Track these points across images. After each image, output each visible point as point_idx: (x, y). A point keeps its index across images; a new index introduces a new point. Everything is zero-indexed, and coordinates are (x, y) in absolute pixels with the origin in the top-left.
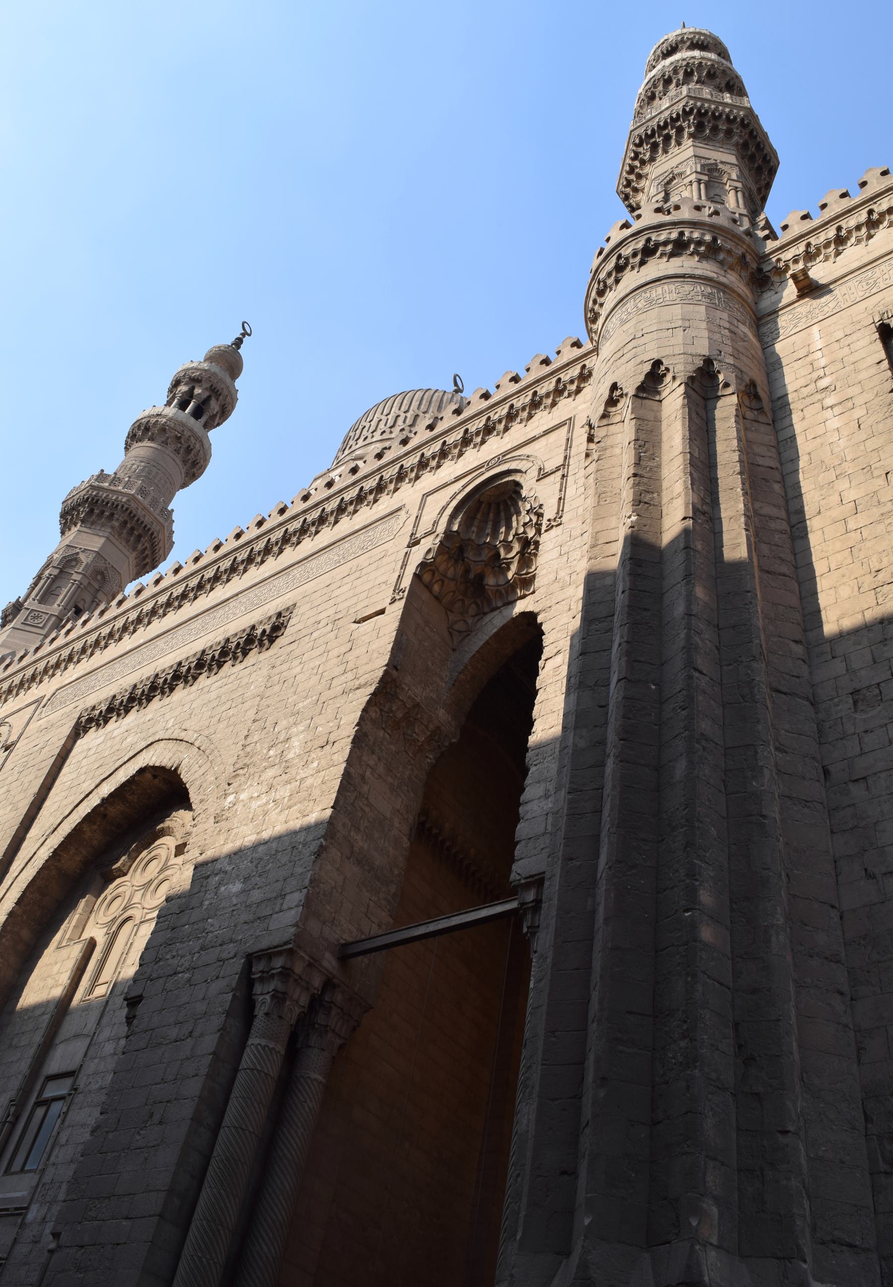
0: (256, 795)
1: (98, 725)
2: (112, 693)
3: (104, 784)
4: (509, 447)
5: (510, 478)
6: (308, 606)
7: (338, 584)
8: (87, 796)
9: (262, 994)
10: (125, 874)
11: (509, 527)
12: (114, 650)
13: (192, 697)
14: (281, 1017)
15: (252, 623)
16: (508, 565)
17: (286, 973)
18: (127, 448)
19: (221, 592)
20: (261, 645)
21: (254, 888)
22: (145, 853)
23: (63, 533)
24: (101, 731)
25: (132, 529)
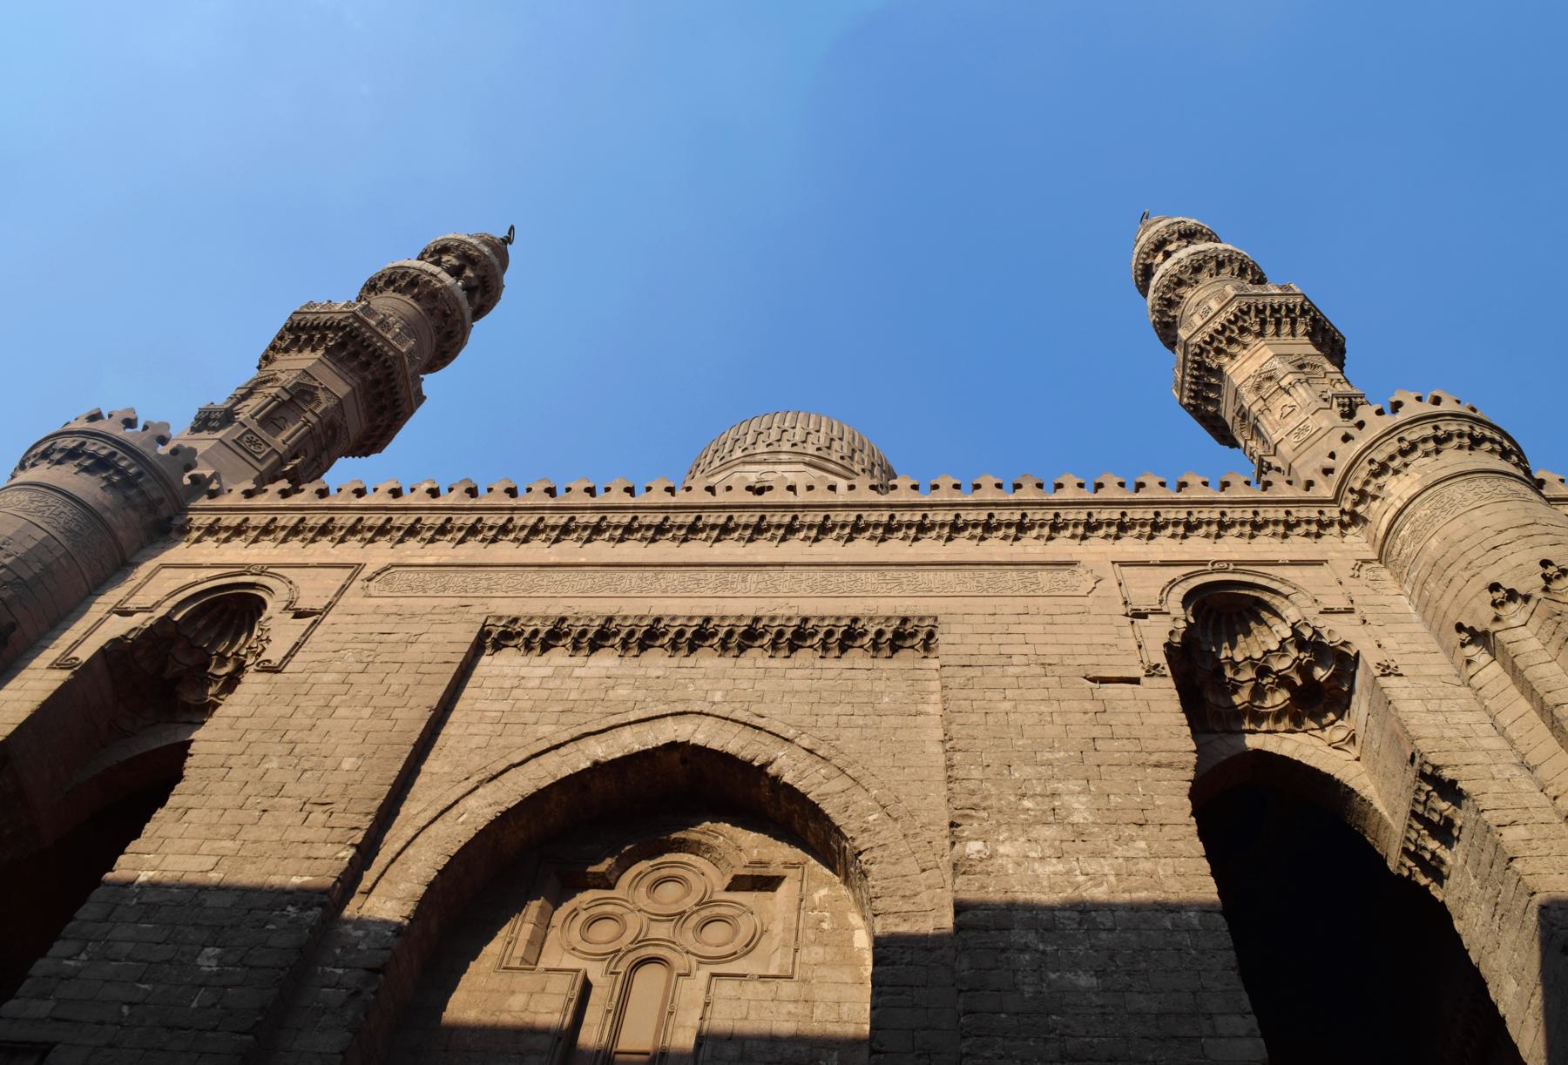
3: (591, 741)
4: (1236, 557)
10: (611, 887)
11: (1232, 647)
16: (1236, 688)
18: (371, 287)
22: (644, 865)
25: (381, 395)
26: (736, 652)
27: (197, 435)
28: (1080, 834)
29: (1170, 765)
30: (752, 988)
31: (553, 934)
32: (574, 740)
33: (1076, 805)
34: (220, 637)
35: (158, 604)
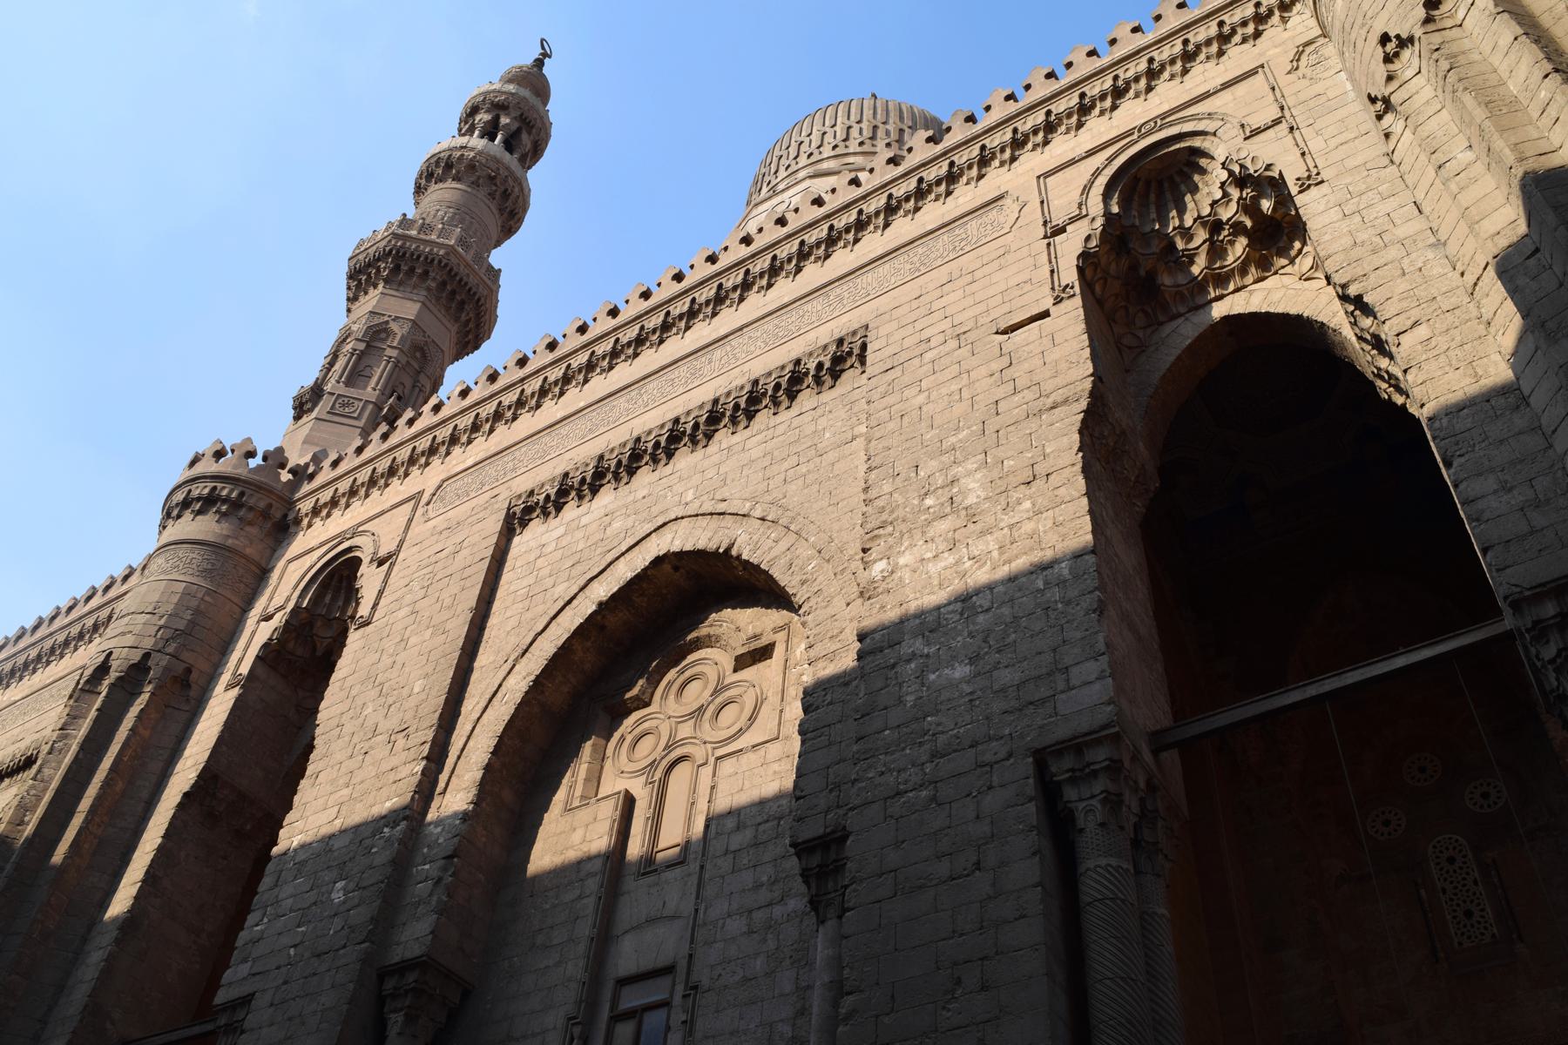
0: (929, 555)
2: (560, 471)
3: (595, 584)
4: (1166, 108)
5: (1182, 145)
6: (894, 325)
7: (938, 293)
8: (569, 602)
9: (1081, 800)
10: (648, 704)
11: (1182, 211)
12: (527, 422)
14: (1122, 828)
15: (794, 355)
17: (1114, 768)
18: (419, 190)
19: (702, 332)
20: (818, 380)
21: (996, 668)
23: (352, 300)
24: (553, 522)
25: (453, 293)
26: (704, 442)
27: (301, 422)
28: (972, 516)
29: (1066, 401)
30: (751, 759)
31: (608, 764)
32: (582, 589)
33: (972, 486)
34: (347, 602)
35: (288, 599)
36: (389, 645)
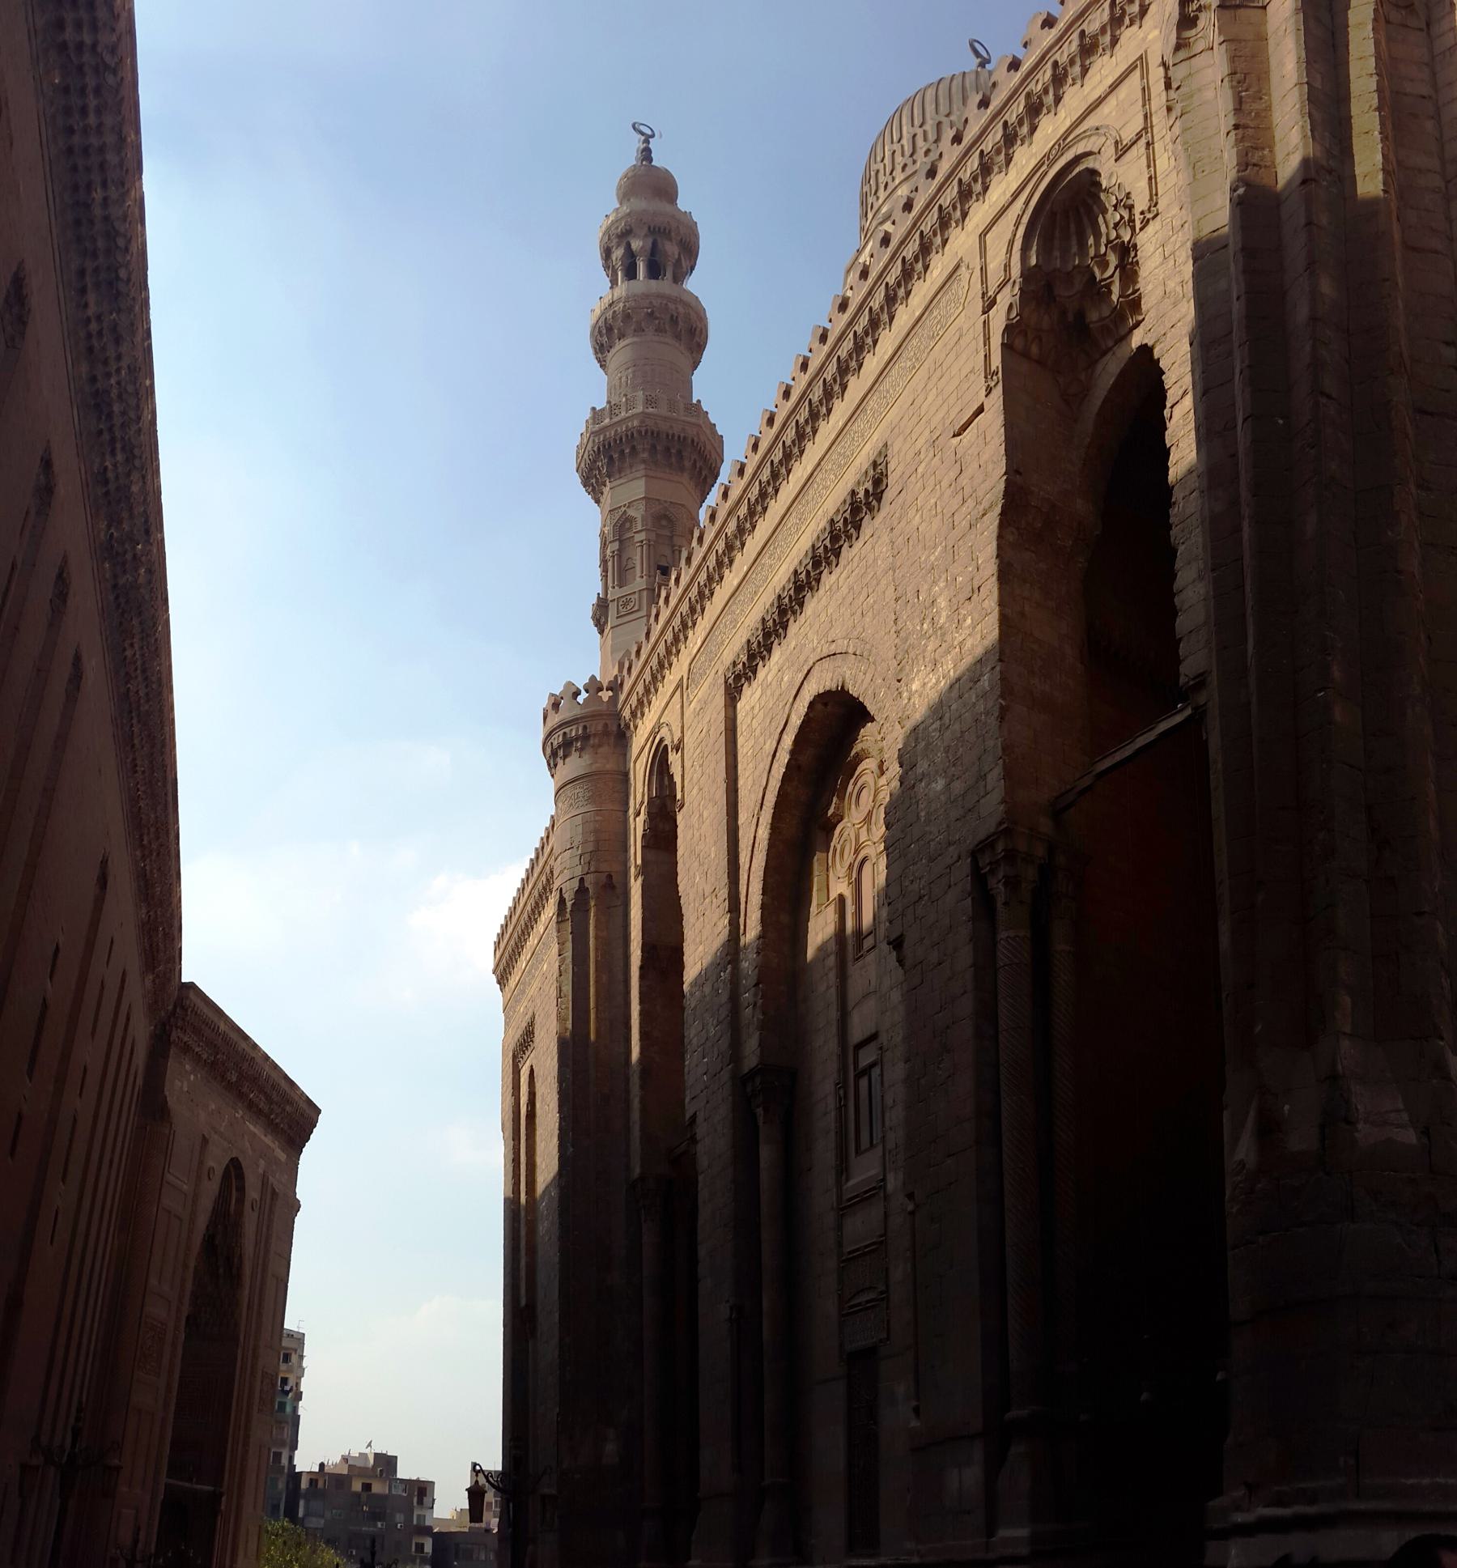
1: (748, 679)
2: (744, 640)
3: (785, 736)
12: (721, 593)
13: (824, 602)
24: (755, 684)
25: (668, 449)
36: (695, 819)
